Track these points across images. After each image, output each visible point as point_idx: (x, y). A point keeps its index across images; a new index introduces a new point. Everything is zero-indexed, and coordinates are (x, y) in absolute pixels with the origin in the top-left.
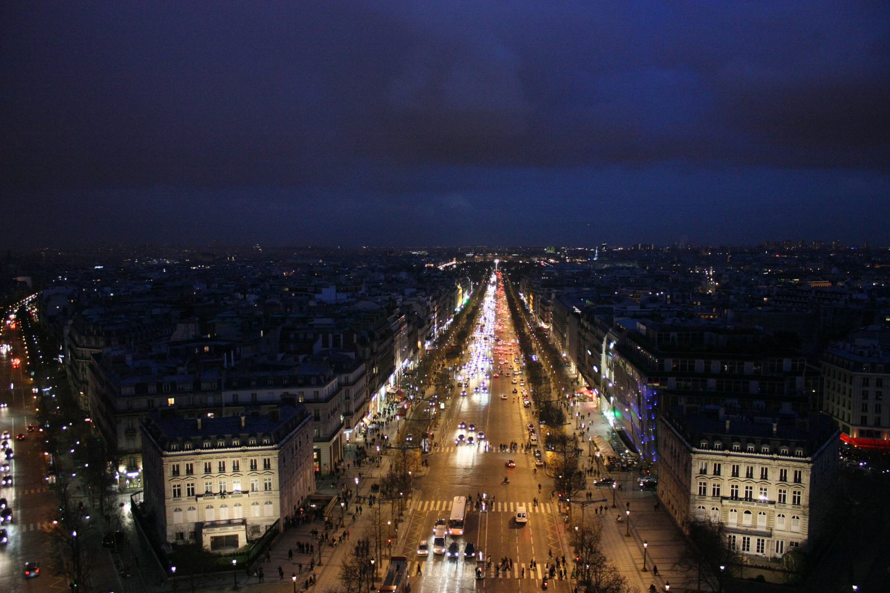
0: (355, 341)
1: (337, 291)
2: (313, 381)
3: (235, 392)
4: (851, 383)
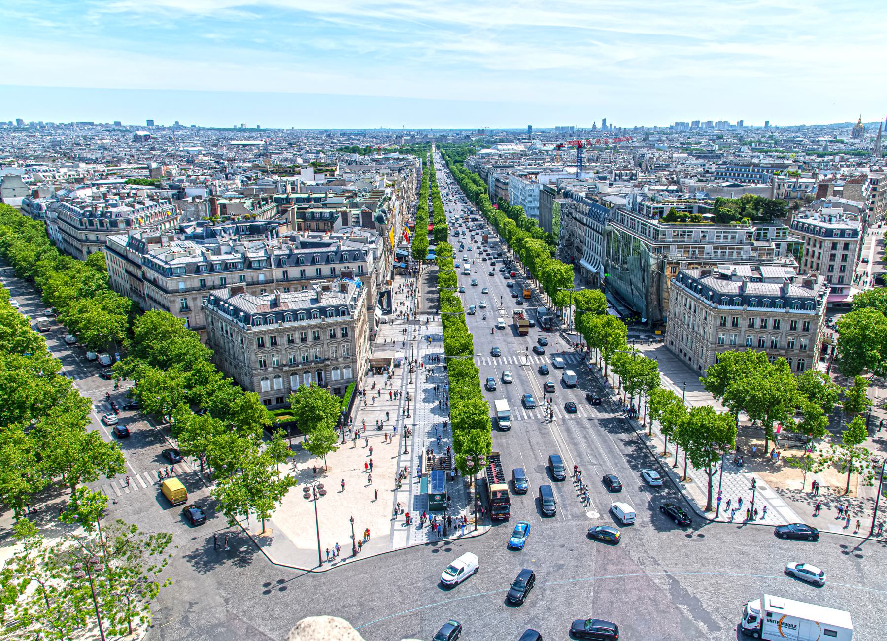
1: (315, 173)
4: (820, 248)
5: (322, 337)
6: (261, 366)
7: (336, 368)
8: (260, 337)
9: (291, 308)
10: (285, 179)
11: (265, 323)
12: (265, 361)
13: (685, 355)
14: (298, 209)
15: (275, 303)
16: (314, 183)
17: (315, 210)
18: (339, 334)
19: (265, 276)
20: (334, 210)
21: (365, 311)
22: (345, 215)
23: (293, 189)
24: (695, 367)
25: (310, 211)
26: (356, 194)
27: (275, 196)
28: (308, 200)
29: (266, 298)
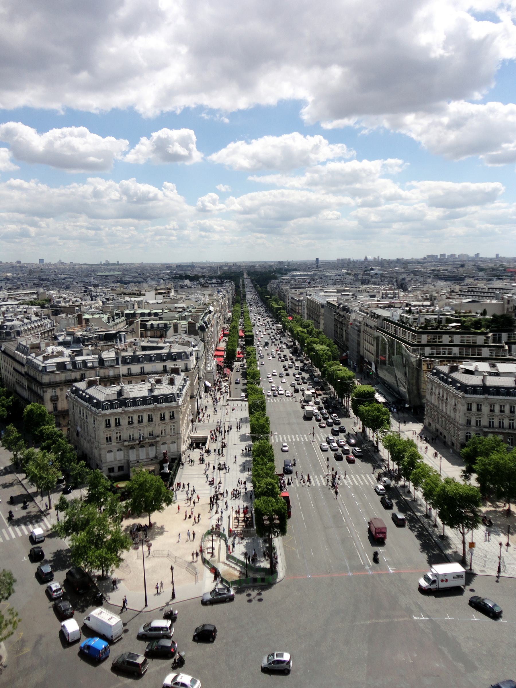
0: (197, 329)
1: (156, 295)
2: (183, 358)
3: (129, 366)
5: (154, 419)
6: (107, 442)
8: (107, 418)
9: (131, 397)
10: (133, 299)
12: (110, 438)
13: (441, 433)
14: (141, 321)
15: (120, 393)
16: (154, 302)
17: (154, 322)
18: (167, 417)
19: (114, 372)
20: (168, 322)
21: (188, 399)
22: (176, 325)
23: (139, 307)
24: (449, 443)
25: (150, 322)
26: (184, 310)
27: (126, 312)
28: (150, 314)
29: (113, 389)
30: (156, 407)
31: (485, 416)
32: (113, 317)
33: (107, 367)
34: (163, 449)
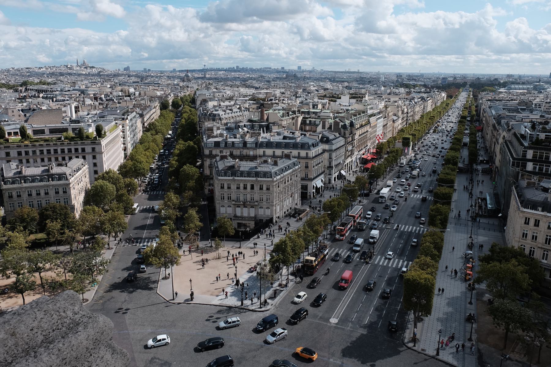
2: (306, 147)
7: (261, 208)
11: (225, 176)
14: (303, 118)
30: (257, 180)
31: (542, 233)
32: (288, 113)
33: (248, 148)
34: (261, 212)
